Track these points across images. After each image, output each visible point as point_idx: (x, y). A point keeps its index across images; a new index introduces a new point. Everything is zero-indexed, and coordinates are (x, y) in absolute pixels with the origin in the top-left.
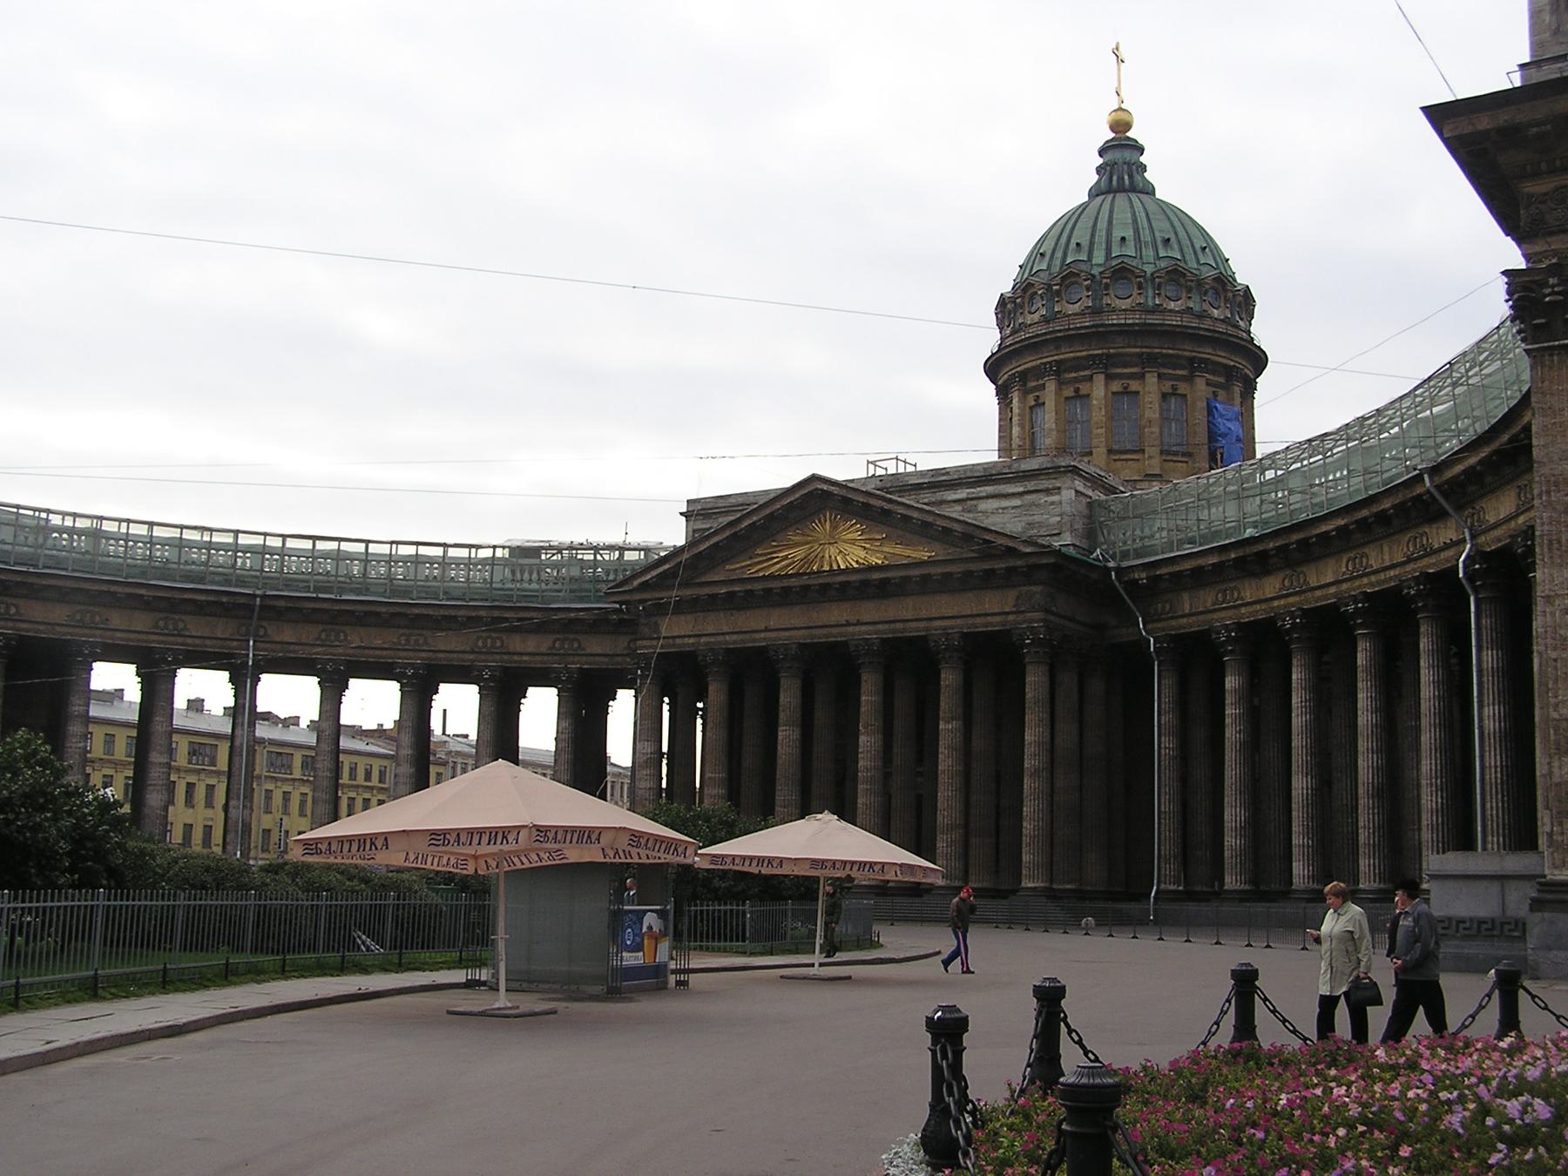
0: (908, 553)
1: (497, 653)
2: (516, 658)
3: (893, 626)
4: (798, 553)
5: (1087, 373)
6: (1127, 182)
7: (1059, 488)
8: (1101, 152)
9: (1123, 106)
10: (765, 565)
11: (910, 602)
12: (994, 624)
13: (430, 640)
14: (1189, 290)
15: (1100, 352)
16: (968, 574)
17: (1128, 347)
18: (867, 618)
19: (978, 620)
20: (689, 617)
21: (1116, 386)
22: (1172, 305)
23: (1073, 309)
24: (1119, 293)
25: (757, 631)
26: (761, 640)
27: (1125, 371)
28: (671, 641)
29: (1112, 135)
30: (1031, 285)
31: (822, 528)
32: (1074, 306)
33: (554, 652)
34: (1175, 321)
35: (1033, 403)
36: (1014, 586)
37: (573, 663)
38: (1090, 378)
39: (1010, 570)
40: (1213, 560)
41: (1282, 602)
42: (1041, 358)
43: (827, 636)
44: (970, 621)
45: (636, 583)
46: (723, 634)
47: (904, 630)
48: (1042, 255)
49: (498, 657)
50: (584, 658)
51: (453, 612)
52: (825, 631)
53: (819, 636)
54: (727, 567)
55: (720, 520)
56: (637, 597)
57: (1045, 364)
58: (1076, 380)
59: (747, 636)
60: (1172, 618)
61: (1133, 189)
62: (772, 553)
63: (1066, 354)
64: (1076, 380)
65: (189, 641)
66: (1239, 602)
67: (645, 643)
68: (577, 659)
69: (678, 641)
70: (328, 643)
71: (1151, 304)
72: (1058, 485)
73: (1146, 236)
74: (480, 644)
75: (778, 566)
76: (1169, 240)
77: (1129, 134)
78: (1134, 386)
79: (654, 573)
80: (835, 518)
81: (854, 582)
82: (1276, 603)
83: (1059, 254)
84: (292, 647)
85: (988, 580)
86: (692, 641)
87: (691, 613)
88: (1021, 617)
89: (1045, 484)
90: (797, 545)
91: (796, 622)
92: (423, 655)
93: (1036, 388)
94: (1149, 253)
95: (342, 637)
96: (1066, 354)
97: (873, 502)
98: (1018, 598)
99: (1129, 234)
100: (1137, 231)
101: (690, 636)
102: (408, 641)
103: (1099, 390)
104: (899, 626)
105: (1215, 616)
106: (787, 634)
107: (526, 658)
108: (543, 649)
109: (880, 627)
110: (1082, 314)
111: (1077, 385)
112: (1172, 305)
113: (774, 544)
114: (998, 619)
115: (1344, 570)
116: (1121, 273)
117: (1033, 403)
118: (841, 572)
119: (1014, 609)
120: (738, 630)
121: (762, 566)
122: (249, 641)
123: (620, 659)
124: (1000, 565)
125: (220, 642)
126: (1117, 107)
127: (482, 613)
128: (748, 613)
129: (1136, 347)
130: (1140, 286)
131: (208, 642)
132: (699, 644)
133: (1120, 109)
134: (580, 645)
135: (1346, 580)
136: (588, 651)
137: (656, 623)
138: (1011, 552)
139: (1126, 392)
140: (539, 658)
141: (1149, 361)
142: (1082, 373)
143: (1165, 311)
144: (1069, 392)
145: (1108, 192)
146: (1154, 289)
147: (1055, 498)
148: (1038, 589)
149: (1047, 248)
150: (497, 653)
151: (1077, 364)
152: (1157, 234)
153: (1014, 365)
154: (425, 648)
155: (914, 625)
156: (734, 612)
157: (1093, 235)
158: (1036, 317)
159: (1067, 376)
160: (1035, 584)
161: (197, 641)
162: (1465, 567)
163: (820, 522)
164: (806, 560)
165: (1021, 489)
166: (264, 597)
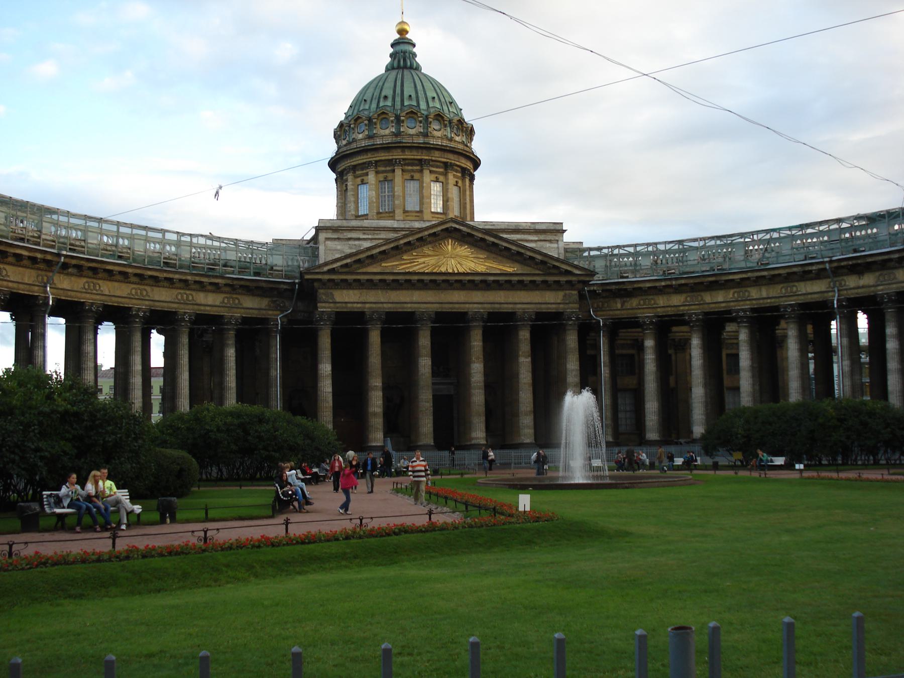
0: (501, 267)
1: (190, 304)
2: (202, 308)
3: (493, 305)
4: (431, 261)
5: (418, 168)
6: (409, 64)
7: (557, 241)
8: (393, 46)
9: (404, 20)
10: (409, 265)
11: (502, 293)
12: (553, 308)
13: (150, 294)
14: (462, 131)
15: (426, 158)
16: (545, 282)
17: (442, 158)
18: (476, 300)
19: (543, 306)
20: (356, 292)
21: (433, 176)
22: (457, 139)
23: (412, 132)
24: (409, 125)
25: (406, 303)
26: (408, 308)
27: (437, 170)
28: (344, 305)
29: (397, 36)
30: (383, 113)
31: (449, 246)
32: (411, 129)
33: (224, 305)
34: (461, 146)
35: (382, 179)
36: (563, 290)
37: (236, 313)
38: (421, 171)
39: (569, 282)
40: (648, 285)
41: (687, 308)
42: (392, 156)
43: (451, 308)
44: (538, 306)
45: (326, 269)
46: (382, 303)
47: (500, 308)
48: (386, 97)
49: (191, 307)
50: (243, 310)
51: (171, 276)
52: (451, 306)
53: (447, 308)
54: (383, 265)
55: (345, 234)
56: (327, 277)
57: (396, 159)
58: (413, 171)
59: (399, 305)
60: (608, 310)
61: (411, 68)
62: (412, 259)
63: (409, 155)
64: (413, 171)
65: (10, 284)
66: (654, 306)
67: (324, 305)
68: (239, 310)
69: (349, 305)
70: (89, 291)
71: (449, 136)
72: (557, 239)
73: (442, 100)
74: (179, 297)
75: (418, 267)
76: (451, 103)
77: (408, 36)
78: (441, 178)
79: (339, 264)
80: (454, 244)
81: (477, 280)
82: (682, 308)
83: (398, 99)
84: (69, 293)
85: (558, 286)
86: (359, 305)
87: (359, 289)
88: (566, 306)
89: (549, 237)
90: (429, 256)
91: (430, 299)
92: (147, 303)
93: (383, 172)
94: (445, 108)
95: (98, 288)
96: (409, 155)
97: (487, 238)
98: (565, 296)
99: (435, 95)
100: (438, 95)
101: (358, 303)
102: (136, 293)
103: (427, 177)
104: (497, 306)
105: (639, 311)
106: (425, 306)
107: (208, 308)
108: (218, 303)
109: (486, 306)
110: (418, 135)
111: (412, 174)
112: (457, 139)
113: (414, 254)
114: (554, 306)
115: (731, 296)
116: (439, 117)
117: (382, 179)
118: (459, 274)
119: (562, 302)
120: (391, 301)
121: (406, 266)
122: (46, 287)
123: (264, 312)
124: (563, 279)
125: (27, 287)
126: (401, 20)
127: (189, 278)
128: (398, 292)
129: (444, 158)
130: (445, 126)
131: (21, 286)
132: (365, 308)
133: (403, 22)
134: (239, 301)
135: (733, 301)
136: (245, 305)
137: (331, 293)
138: (568, 273)
139: (437, 180)
140: (215, 309)
141: (447, 166)
142: (415, 168)
143: (455, 141)
144: (407, 176)
145: (399, 67)
146: (451, 128)
147: (555, 245)
148: (575, 292)
149: (388, 91)
150: (190, 304)
151: (412, 162)
152: (446, 99)
153: (368, 157)
154: (147, 298)
155: (506, 306)
156: (388, 291)
157: (394, 91)
158: (387, 132)
159: (407, 168)
160: (574, 290)
161: (15, 285)
162: (837, 303)
163: (445, 245)
164: (435, 266)
165: (537, 239)
166: (66, 256)
